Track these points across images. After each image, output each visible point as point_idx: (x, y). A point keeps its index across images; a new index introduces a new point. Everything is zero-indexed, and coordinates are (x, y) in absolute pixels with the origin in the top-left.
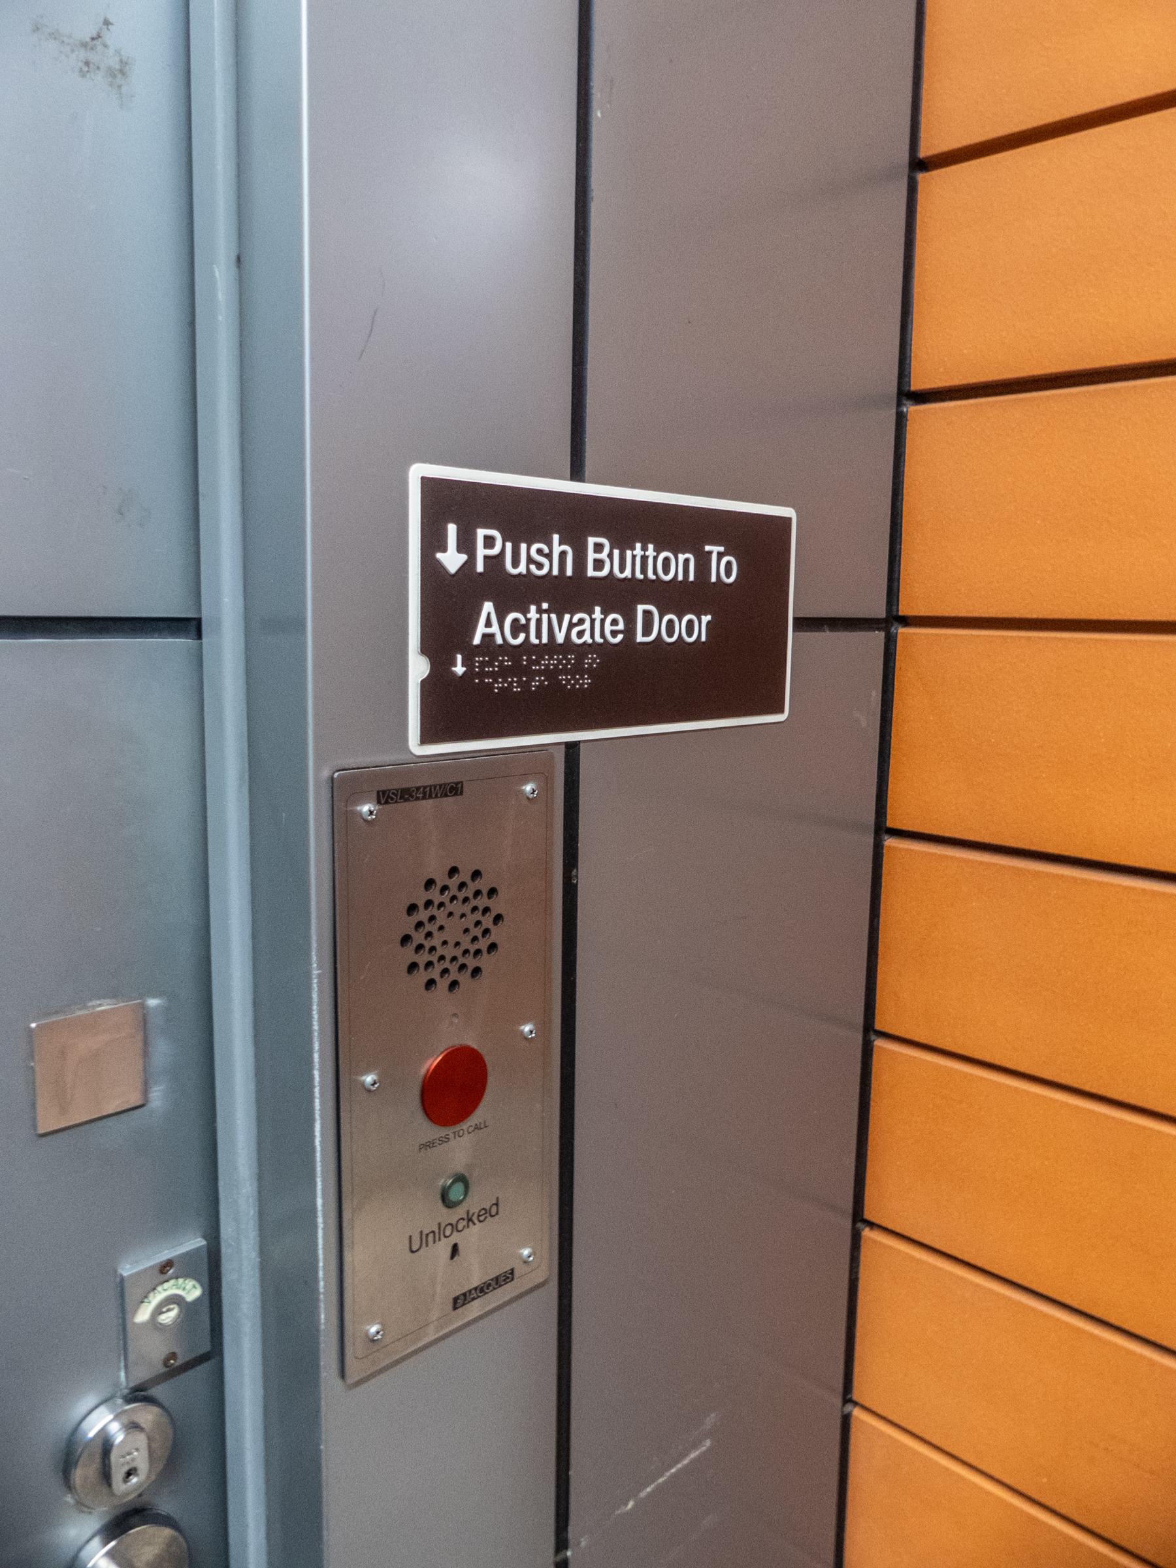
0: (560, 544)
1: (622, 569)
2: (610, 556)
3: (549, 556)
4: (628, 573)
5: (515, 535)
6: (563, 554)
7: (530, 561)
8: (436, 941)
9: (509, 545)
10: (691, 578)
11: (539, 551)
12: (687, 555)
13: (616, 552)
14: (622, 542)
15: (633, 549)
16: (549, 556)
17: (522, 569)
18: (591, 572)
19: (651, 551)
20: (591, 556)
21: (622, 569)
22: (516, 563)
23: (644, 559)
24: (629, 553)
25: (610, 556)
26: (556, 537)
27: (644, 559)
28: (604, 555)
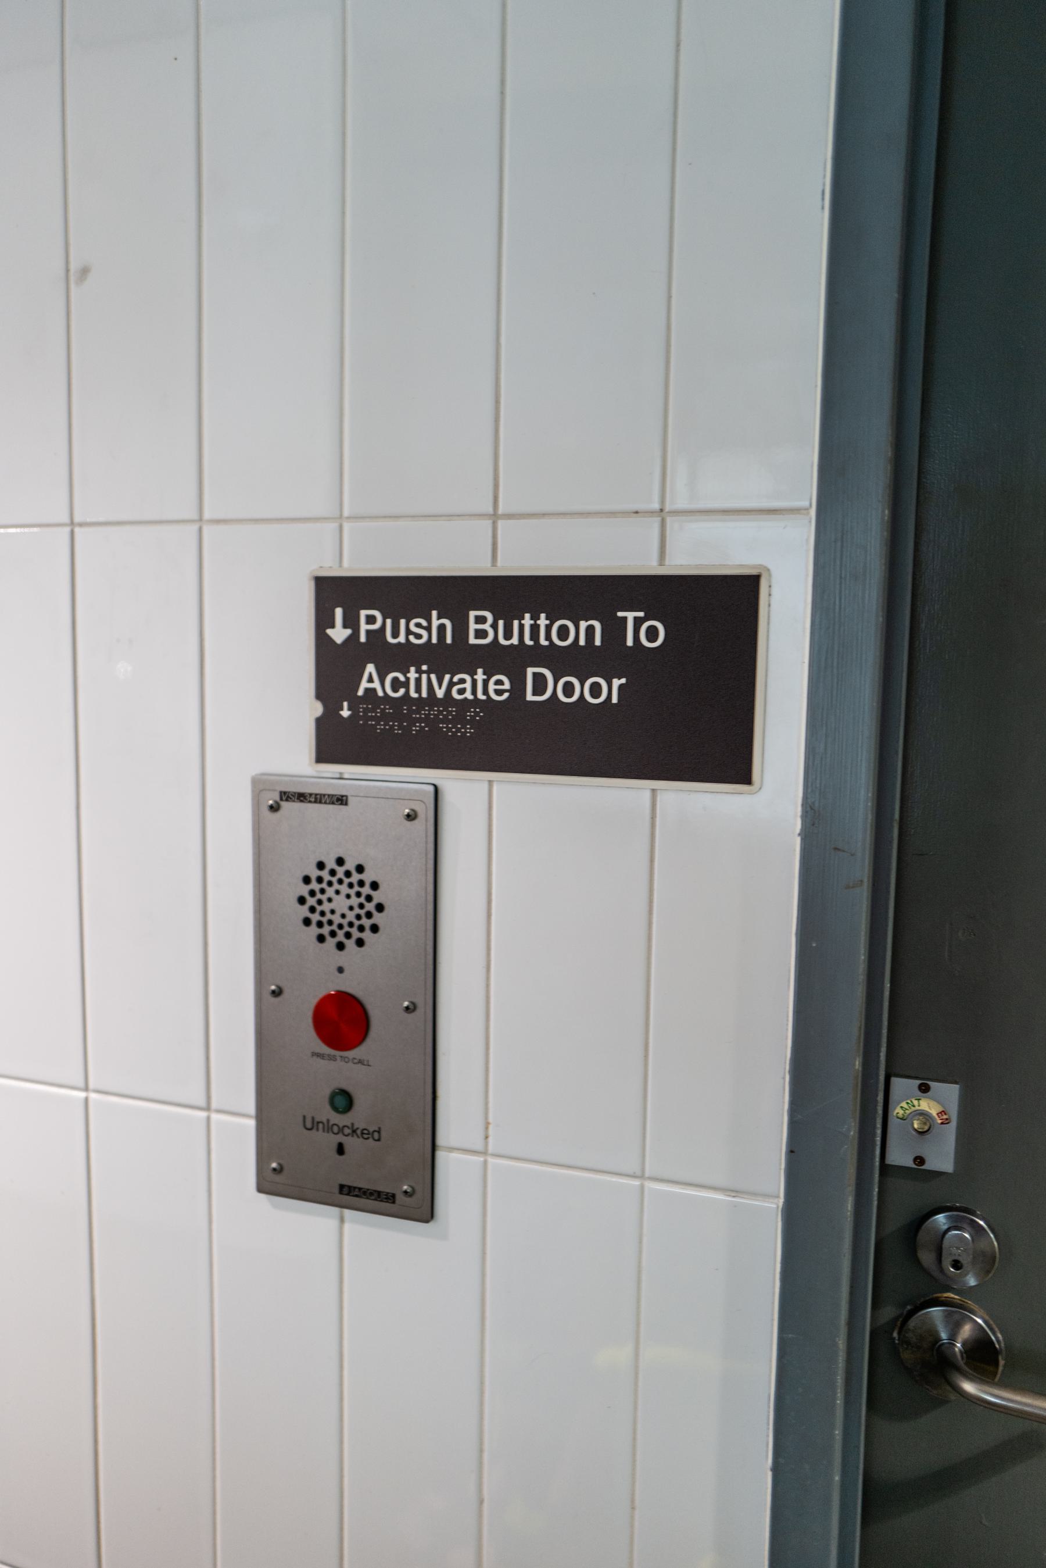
1: (508, 635)
2: (495, 626)
5: (393, 613)
6: (442, 628)
7: (409, 632)
9: (389, 622)
13: (501, 623)
14: (507, 613)
16: (429, 629)
17: (402, 639)
18: (472, 640)
19: (543, 621)
20: (473, 627)
21: (508, 635)
22: (395, 635)
23: (535, 629)
24: (516, 623)
25: (495, 626)
26: (434, 613)
27: (535, 629)
28: (486, 626)
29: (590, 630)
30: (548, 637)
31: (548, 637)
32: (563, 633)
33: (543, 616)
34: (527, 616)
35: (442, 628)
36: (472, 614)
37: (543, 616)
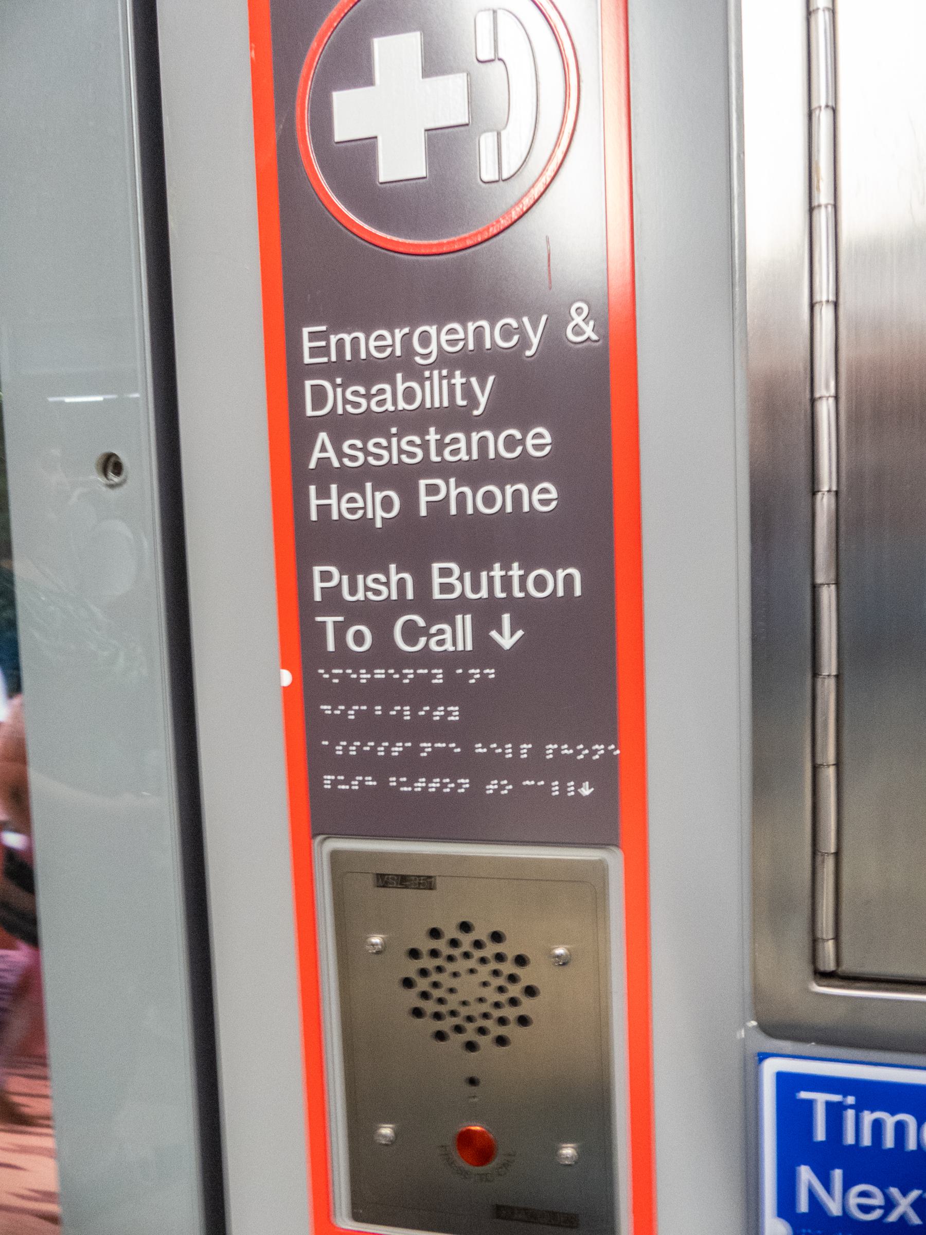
0: (397, 573)
1: (476, 588)
2: (461, 579)
3: (387, 584)
4: (484, 593)
5: (351, 569)
6: (401, 583)
7: (367, 588)
8: (484, 972)
9: (345, 578)
10: (578, 592)
11: (376, 581)
12: (571, 570)
13: (467, 575)
14: (475, 563)
15: (490, 569)
16: (387, 584)
17: (360, 596)
18: (437, 595)
19: (516, 572)
20: (437, 581)
21: (476, 588)
23: (507, 582)
24: (484, 575)
25: (461, 579)
27: (507, 582)
29: (569, 579)
30: (523, 587)
31: (523, 587)
32: (540, 583)
33: (515, 565)
34: (497, 566)
35: (401, 583)
36: (436, 567)
37: (515, 565)
